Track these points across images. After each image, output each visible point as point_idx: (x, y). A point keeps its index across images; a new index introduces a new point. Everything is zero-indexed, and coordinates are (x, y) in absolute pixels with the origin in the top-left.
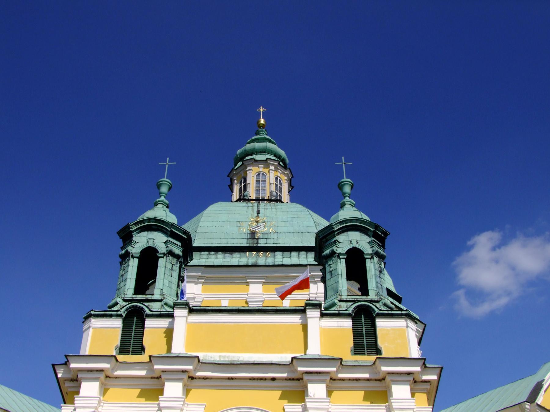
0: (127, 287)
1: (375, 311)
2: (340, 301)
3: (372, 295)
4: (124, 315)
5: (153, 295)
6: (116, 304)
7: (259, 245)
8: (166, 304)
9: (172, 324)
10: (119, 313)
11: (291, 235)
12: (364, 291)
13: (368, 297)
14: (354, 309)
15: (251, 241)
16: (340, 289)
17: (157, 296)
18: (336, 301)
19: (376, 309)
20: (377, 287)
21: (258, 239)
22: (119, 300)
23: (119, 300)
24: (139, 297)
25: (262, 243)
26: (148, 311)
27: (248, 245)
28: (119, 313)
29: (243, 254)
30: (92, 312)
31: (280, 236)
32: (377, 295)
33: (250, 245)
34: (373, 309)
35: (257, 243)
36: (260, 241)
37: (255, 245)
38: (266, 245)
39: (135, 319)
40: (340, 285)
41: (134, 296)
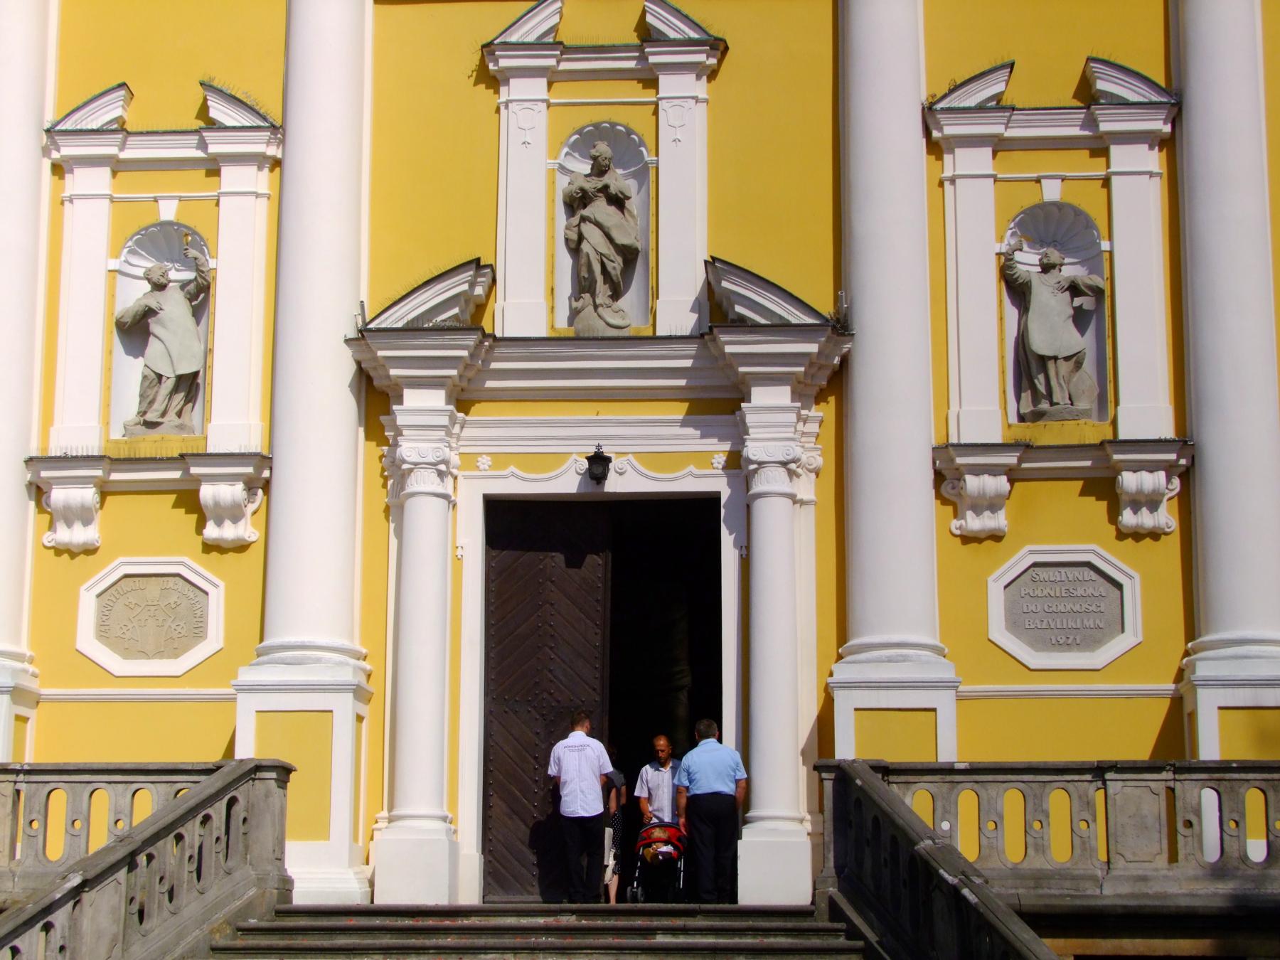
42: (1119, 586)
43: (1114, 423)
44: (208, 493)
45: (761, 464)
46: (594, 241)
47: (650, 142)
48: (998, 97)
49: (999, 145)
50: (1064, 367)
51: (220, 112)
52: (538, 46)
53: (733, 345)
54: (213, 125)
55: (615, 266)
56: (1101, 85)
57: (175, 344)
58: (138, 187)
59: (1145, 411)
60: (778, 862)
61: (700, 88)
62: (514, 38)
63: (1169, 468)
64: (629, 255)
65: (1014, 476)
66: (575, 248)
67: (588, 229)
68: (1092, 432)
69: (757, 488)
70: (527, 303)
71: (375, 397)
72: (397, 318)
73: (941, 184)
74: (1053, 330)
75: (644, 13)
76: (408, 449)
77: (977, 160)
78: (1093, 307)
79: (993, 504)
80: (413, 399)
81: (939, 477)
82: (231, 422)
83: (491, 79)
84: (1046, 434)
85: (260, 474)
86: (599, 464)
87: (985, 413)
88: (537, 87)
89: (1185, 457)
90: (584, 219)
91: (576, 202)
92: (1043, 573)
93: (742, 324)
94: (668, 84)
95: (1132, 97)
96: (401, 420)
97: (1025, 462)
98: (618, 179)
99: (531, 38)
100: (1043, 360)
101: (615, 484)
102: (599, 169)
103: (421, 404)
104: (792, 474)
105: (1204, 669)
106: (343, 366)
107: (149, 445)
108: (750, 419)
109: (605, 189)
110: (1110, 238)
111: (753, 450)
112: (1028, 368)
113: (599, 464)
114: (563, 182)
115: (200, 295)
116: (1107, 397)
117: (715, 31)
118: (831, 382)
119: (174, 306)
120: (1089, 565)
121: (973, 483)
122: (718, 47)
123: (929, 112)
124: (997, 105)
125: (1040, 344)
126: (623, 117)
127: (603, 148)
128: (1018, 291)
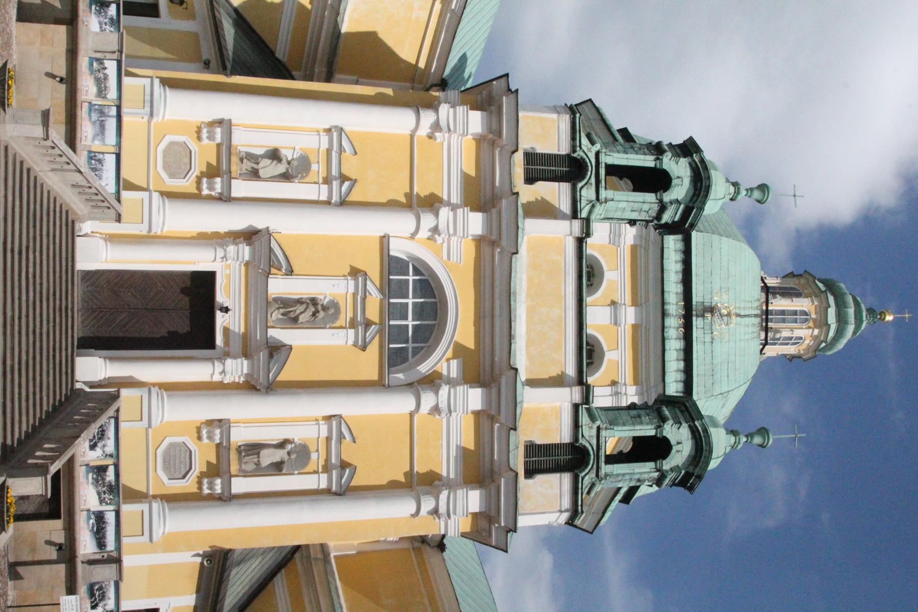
0: (616, 155)
1: (581, 472)
2: (599, 428)
3: (605, 469)
4: (575, 155)
5: (606, 188)
6: (593, 143)
7: (694, 318)
8: (593, 206)
9: (563, 217)
10: (578, 149)
11: (708, 360)
12: (612, 459)
13: (603, 464)
14: (584, 446)
15: (700, 308)
16: (615, 428)
17: (603, 194)
18: (598, 423)
19: (583, 474)
20: (618, 475)
21: (703, 316)
22: (598, 146)
23: (598, 146)
24: (602, 172)
25: (697, 322)
26: (580, 185)
27: (694, 303)
28: (578, 149)
29: (681, 297)
30: (578, 115)
31: (708, 346)
32: (606, 475)
33: (694, 307)
34: (584, 470)
35: (697, 316)
36: (700, 319)
37: (694, 313)
38: (694, 328)
39: (571, 169)
40: (620, 428)
41: (603, 165)
42: (184, 477)
43: (237, 476)
44: (218, 180)
45: (224, 364)
46: (300, 308)
47: (334, 325)
48: (344, 438)
49: (328, 439)
50: (256, 460)
51: (347, 184)
52: (365, 290)
53: (263, 355)
54: (342, 183)
55: (292, 315)
56: (348, 471)
57: (268, 168)
58: (323, 157)
59: (240, 485)
60: (92, 369)
61: (350, 342)
62: (368, 282)
63: (222, 493)
64: (295, 320)
65: (218, 446)
66: (299, 302)
67: (304, 306)
68: (234, 468)
69: (216, 363)
70: (279, 286)
71: (250, 236)
72: (274, 245)
73: (317, 420)
74: (268, 457)
75: (375, 324)
76: (231, 249)
77: (324, 433)
78: (278, 468)
79: (210, 438)
80: (247, 249)
81: (220, 421)
82: (240, 188)
83: (355, 272)
84: (233, 456)
85: (225, 198)
86: (226, 310)
87: (240, 436)
88: (351, 290)
89: (227, 498)
90: (308, 304)
91: (314, 301)
92: (188, 454)
93: (271, 356)
94: (351, 332)
95: (343, 481)
96: (241, 246)
97: (222, 449)
98: (322, 314)
99: (368, 287)
100: (259, 453)
101: (219, 315)
102: (325, 308)
103: (246, 251)
104: (221, 373)
105: (155, 505)
106: (260, 225)
107: (234, 159)
108: (239, 360)
109: (318, 312)
110: (299, 474)
111: (229, 362)
112: (254, 448)
113: (226, 310)
114: (322, 297)
115: (286, 177)
116: (246, 474)
117: (368, 347)
118: (250, 387)
119: (281, 168)
120: (190, 468)
121: (218, 431)
122: (364, 348)
123: (340, 417)
124: (341, 437)
125: (264, 453)
126: (342, 316)
127: (332, 311)
128: (282, 445)
